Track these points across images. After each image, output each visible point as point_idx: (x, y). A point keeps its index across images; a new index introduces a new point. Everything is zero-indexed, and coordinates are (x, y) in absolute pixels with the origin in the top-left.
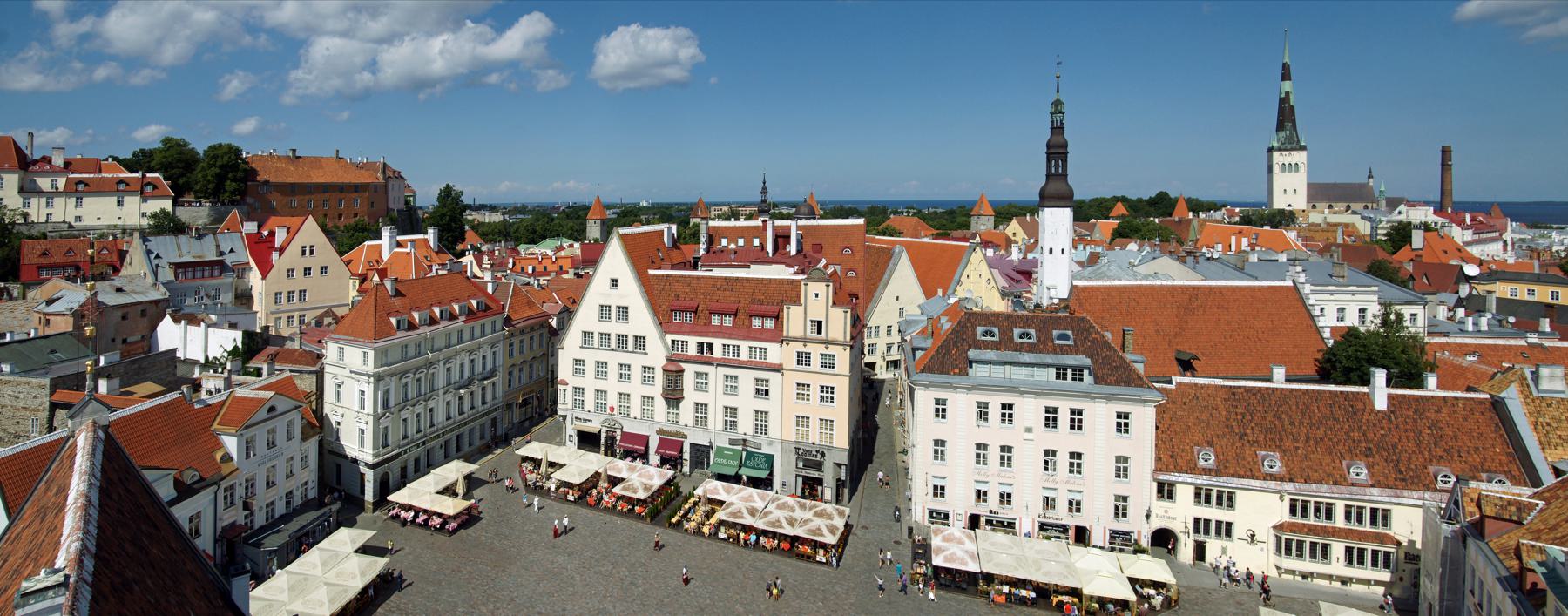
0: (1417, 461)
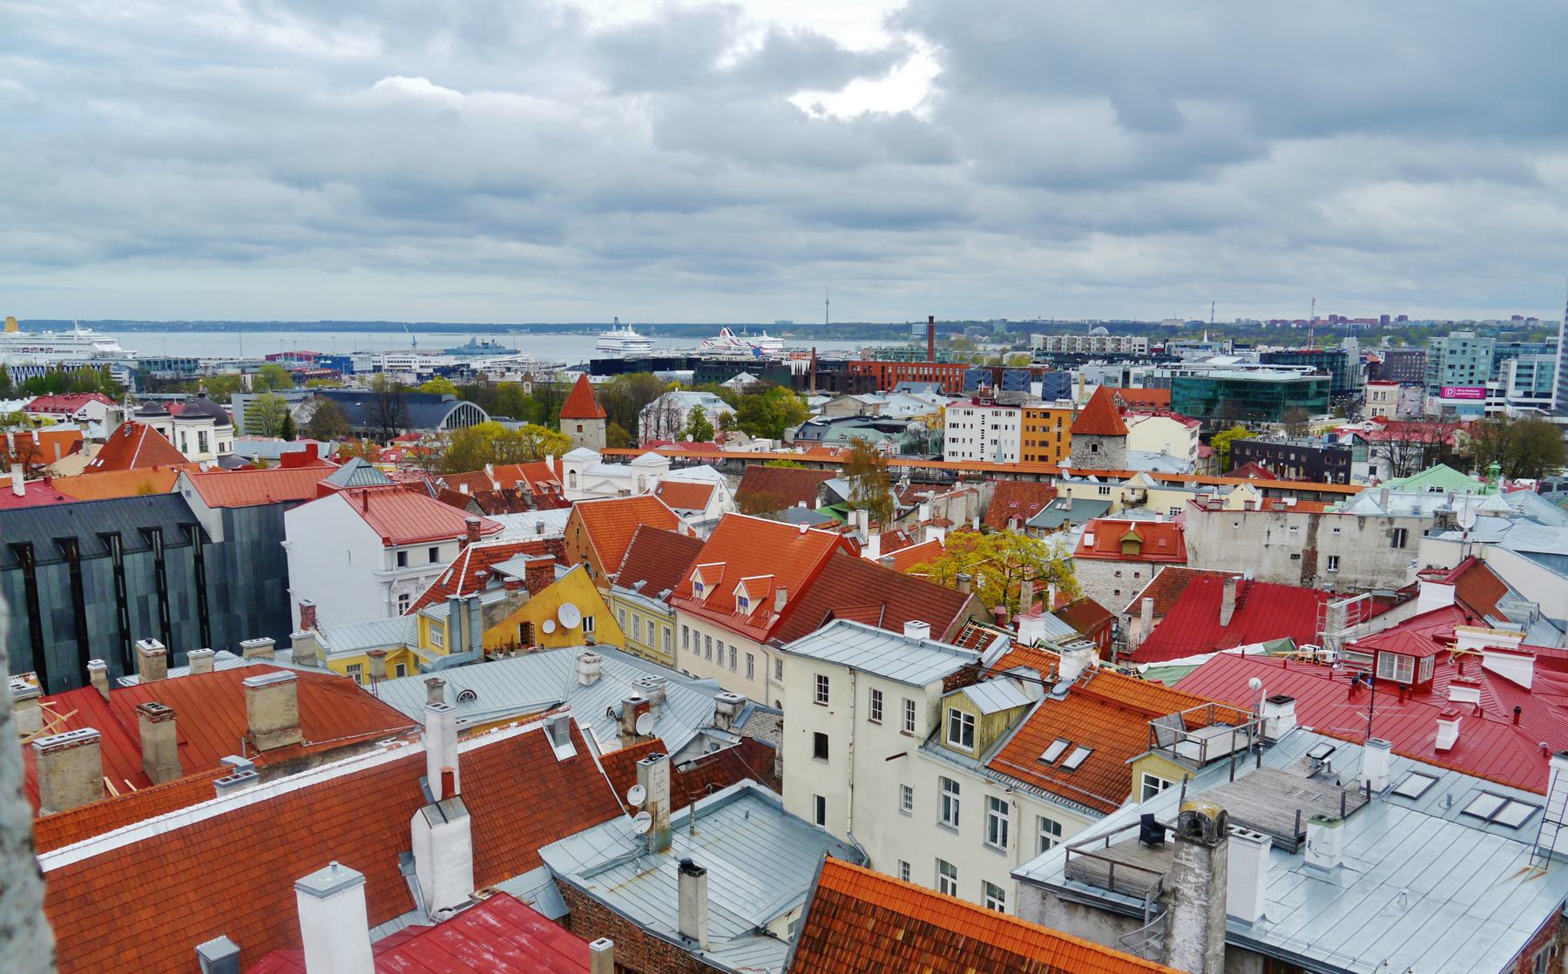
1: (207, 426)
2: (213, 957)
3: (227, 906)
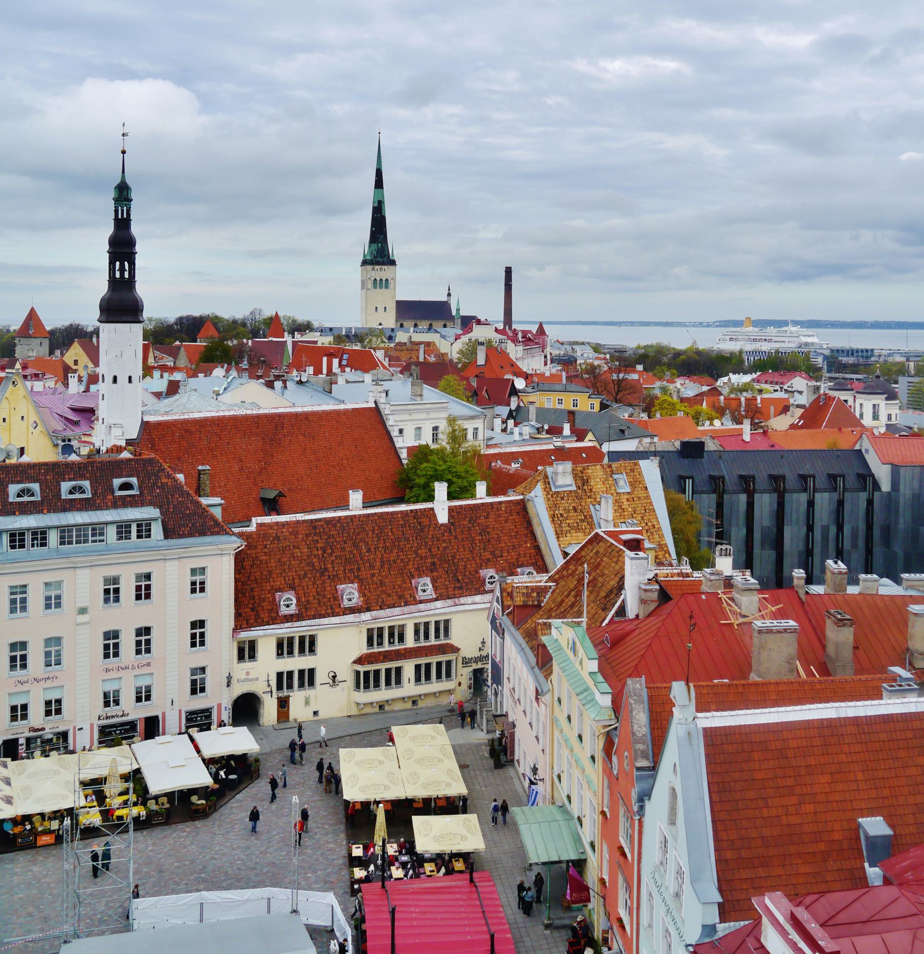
0: (471, 567)
1: (880, 400)
3: (886, 792)
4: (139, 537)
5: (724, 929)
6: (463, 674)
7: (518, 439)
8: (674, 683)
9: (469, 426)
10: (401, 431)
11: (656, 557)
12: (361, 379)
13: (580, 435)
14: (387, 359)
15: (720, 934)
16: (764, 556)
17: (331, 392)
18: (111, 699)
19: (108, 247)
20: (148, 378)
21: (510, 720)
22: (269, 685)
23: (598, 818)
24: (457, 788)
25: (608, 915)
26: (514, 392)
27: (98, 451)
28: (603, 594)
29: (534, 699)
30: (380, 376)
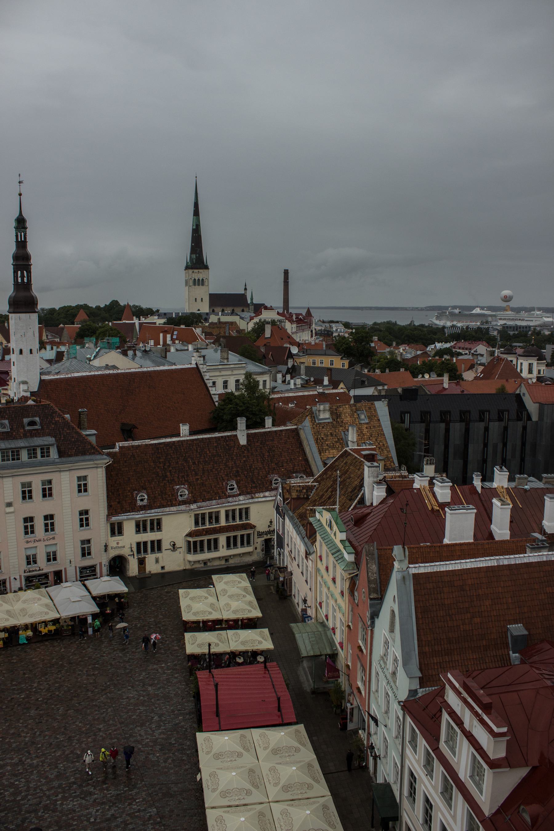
2: (515, 633)
4: (42, 457)
5: (421, 692)
6: (259, 542)
7: (293, 388)
8: (395, 546)
9: (260, 379)
10: (214, 383)
11: (385, 465)
12: (186, 348)
13: (334, 384)
14: (204, 334)
15: (420, 695)
16: (455, 464)
17: (166, 357)
18: (31, 560)
19: (12, 261)
20: (43, 350)
21: (289, 570)
22: (132, 551)
23: (345, 629)
24: (257, 613)
25: (351, 686)
26: (291, 355)
27: (13, 400)
28: (350, 490)
29: (304, 557)
30: (199, 346)
